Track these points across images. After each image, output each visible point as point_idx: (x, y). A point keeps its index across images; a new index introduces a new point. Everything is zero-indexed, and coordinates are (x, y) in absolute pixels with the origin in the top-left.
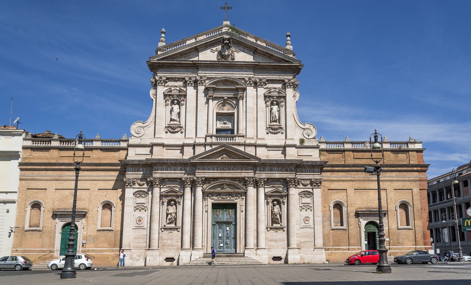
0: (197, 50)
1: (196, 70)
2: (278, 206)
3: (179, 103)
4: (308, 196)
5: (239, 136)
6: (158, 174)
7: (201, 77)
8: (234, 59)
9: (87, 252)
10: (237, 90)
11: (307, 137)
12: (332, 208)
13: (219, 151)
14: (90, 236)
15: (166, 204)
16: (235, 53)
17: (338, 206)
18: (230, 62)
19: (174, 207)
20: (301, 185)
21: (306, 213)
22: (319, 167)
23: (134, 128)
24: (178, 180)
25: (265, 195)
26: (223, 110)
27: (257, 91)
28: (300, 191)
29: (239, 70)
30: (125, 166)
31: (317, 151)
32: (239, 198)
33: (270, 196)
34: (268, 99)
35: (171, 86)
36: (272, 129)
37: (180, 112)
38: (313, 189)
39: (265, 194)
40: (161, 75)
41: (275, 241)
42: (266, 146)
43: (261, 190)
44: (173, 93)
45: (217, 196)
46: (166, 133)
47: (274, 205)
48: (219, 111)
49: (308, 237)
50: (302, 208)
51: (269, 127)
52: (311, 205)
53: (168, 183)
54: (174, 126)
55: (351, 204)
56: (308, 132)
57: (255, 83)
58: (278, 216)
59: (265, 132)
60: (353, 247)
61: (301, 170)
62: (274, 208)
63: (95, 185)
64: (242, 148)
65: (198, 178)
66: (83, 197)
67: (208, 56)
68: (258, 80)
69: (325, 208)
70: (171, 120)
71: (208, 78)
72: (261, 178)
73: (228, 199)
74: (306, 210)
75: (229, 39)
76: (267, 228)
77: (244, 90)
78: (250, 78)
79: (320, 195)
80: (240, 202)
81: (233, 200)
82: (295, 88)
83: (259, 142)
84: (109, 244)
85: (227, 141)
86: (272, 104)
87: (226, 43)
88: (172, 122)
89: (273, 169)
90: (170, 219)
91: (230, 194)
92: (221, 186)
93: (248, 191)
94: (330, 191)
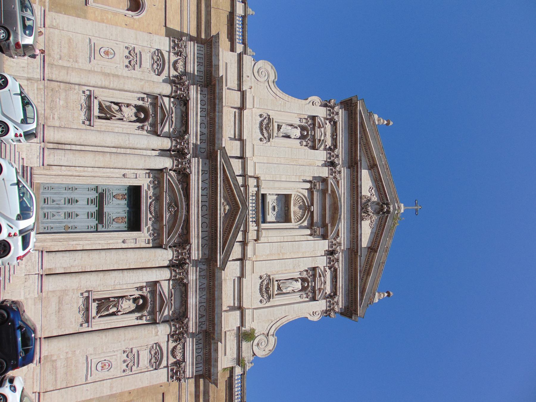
1: (347, 165)
2: (133, 306)
5: (258, 231)
6: (194, 95)
10: (324, 225)
11: (256, 342)
13: (235, 199)
15: (140, 103)
16: (369, 221)
19: (134, 118)
20: (174, 344)
22: (206, 371)
23: (266, 67)
24: (184, 128)
25: (156, 283)
26: (294, 205)
27: (322, 256)
28: (162, 345)
30: (208, 45)
32: (150, 235)
33: (153, 292)
34: (311, 273)
35: (325, 129)
36: (268, 284)
39: (158, 282)
40: (341, 116)
43: (166, 274)
44: (317, 130)
45: (154, 194)
46: (261, 116)
47: (135, 300)
48: (292, 199)
50: (128, 352)
51: (270, 279)
52: (134, 368)
53: (179, 110)
54: (271, 128)
56: (263, 344)
58: (114, 310)
59: (262, 274)
64: (240, 238)
65: (189, 162)
68: (336, 256)
71: (338, 182)
72: (187, 273)
73: (149, 216)
74: (125, 361)
75: (388, 212)
76: (88, 292)
77: (324, 237)
80: (144, 236)
81: (147, 225)
82: (326, 312)
83: (248, 264)
85: (250, 212)
86: (304, 280)
87: (382, 209)
89: (204, 293)
90: (109, 108)
91: (158, 218)
92: (174, 203)
93: (165, 251)
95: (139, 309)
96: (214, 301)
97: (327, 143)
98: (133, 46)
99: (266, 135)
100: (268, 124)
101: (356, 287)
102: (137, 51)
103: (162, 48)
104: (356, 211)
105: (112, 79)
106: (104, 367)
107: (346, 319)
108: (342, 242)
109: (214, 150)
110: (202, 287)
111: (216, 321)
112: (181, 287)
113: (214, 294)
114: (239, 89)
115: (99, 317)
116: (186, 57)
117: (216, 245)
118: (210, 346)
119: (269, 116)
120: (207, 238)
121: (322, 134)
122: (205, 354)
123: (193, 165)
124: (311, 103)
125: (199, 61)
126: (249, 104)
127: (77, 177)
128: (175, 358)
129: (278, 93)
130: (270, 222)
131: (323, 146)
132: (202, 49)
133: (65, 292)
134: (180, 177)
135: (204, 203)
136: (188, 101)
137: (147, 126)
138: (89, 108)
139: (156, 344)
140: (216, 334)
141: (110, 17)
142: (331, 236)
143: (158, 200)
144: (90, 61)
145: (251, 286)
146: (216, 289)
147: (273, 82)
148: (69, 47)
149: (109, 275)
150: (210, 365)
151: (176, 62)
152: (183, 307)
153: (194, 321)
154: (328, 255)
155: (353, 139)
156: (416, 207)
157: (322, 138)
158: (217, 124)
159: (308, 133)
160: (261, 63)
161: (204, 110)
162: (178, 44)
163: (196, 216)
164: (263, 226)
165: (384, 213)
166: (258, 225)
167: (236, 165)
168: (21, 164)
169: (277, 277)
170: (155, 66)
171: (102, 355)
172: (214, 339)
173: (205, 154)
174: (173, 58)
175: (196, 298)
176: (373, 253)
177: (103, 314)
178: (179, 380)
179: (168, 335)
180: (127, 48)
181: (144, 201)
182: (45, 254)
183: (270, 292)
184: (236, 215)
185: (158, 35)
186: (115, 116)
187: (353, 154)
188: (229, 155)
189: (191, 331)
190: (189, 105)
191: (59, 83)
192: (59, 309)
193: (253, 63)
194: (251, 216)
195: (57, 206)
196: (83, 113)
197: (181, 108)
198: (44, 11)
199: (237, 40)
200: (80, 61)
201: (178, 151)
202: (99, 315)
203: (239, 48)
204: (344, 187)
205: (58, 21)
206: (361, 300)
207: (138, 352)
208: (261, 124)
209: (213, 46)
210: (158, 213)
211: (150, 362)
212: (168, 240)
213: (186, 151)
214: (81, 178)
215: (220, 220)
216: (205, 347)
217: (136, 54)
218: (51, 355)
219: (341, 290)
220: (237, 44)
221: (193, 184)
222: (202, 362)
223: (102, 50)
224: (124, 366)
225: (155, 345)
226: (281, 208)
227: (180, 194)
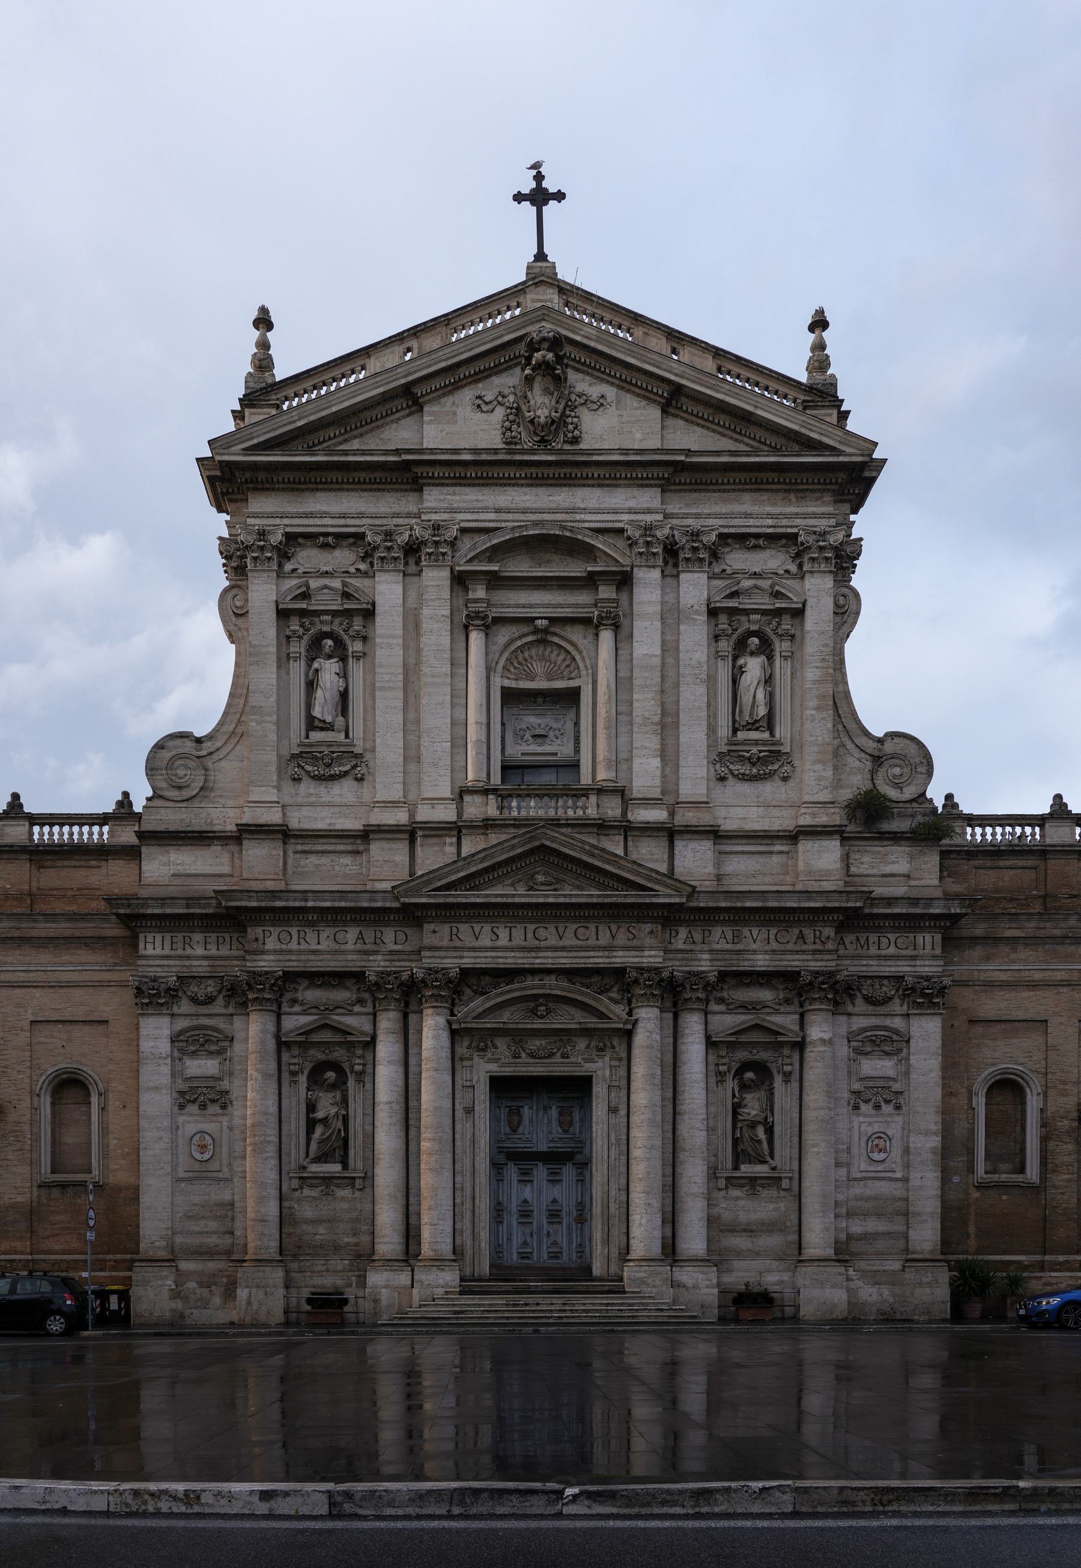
1: (412, 497)
3: (340, 653)
4: (887, 1049)
7: (437, 527)
8: (576, 440)
10: (591, 581)
12: (982, 1100)
15: (303, 1079)
17: (1007, 1087)
18: (560, 451)
20: (859, 1001)
24: (349, 983)
28: (855, 1027)
31: (931, 861)
36: (742, 759)
37: (346, 690)
38: (908, 1015)
39: (708, 1038)
41: (749, 1230)
42: (715, 834)
43: (693, 1026)
46: (297, 780)
47: (744, 1087)
49: (879, 1215)
52: (897, 1087)
55: (1064, 1083)
56: (897, 771)
57: (671, 551)
60: (1061, 1258)
61: (863, 937)
62: (742, 1099)
67: (464, 425)
69: (953, 1100)
70: (312, 724)
71: (464, 531)
73: (557, 1059)
74: (877, 1107)
77: (624, 581)
79: (939, 1044)
81: (578, 1064)
86: (741, 647)
88: (316, 736)
90: (321, 1142)
94: (978, 1029)
98: (175, 1095)
100: (315, 759)
102: (182, 1086)
106: (880, 1146)
112: (726, 987)
115: (772, 1158)
116: (178, 977)
119: (293, 756)
121: (326, 587)
122: (894, 929)
123: (438, 960)
124: (240, 622)
125: (180, 945)
127: (477, 1201)
128: (891, 998)
132: (150, 938)
133: (712, 1221)
134: (468, 991)
139: (849, 1041)
144: (226, 1180)
145: (744, 807)
149: (684, 1139)
151: (194, 1000)
153: (810, 957)
154: (676, 565)
161: (302, 934)
163: (560, 954)
167: (433, 857)
169: (724, 730)
170: (213, 1048)
171: (855, 1151)
173: (408, 931)
174: (185, 1006)
176: (684, 400)
177: (767, 1152)
178: (942, 991)
179: (833, 1014)
180: (182, 1107)
181: (525, 1069)
186: (339, 1130)
191: (284, 1236)
192: (745, 1230)
196: (341, 1193)
197: (301, 988)
200: (228, 1198)
201: (406, 994)
202: (768, 1159)
207: (861, 1079)
211: (887, 1054)
213: (405, 976)
214: (477, 1195)
216: (877, 929)
218: (836, 1243)
219: (785, 522)
223: (198, 1156)
224: (887, 1109)
225: (853, 1044)
227: (509, 991)
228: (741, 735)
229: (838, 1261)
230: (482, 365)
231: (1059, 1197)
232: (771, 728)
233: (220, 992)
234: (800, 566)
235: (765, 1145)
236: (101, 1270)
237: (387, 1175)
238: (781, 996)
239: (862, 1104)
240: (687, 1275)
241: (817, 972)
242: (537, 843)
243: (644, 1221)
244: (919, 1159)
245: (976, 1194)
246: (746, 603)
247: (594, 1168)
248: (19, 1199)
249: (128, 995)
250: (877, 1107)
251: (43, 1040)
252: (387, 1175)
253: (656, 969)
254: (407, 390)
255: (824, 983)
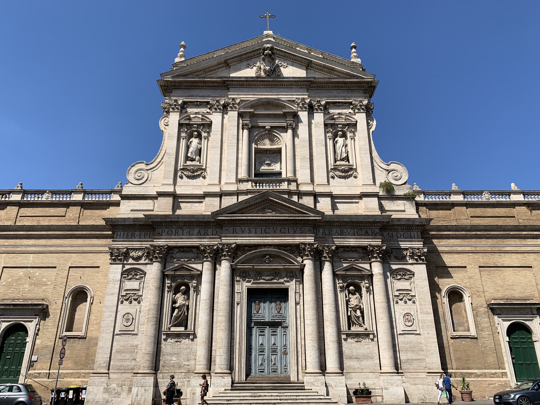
0: (228, 65)
2: (357, 295)
3: (199, 136)
9: (36, 377)
10: (285, 115)
14: (46, 347)
21: (405, 306)
24: (194, 250)
29: (286, 89)
36: (339, 170)
49: (412, 351)
52: (412, 293)
56: (395, 175)
61: (390, 233)
62: (350, 298)
63: (66, 260)
64: (295, 198)
66: (44, 280)
68: (314, 103)
70: (187, 158)
74: (406, 302)
75: (272, 49)
78: (303, 99)
80: (292, 285)
81: (282, 283)
84: (75, 363)
85: (271, 188)
88: (189, 163)
89: (345, 230)
90: (177, 318)
91: (276, 274)
95: (358, 289)
96: (352, 222)
97: (205, 112)
99: (199, 173)
101: (345, 83)
102: (124, 293)
103: (120, 271)
104: (271, 83)
105: (151, 316)
107: (376, 91)
108: (301, 97)
109: (214, 222)
110: (339, 232)
111: (372, 220)
112: (339, 252)
113: (346, 222)
114: (156, 198)
116: (127, 249)
117: (301, 220)
118: (395, 225)
120: (295, 228)
121: (196, 117)
124: (166, 127)
126: (170, 189)
129: (158, 160)
130: (281, 169)
131: (207, 116)
132: (119, 234)
134: (240, 253)
135: (263, 231)
136: (169, 246)
137: (194, 283)
138: (178, 335)
140: (383, 220)
141: (94, 317)
142: (294, 108)
143: (260, 273)
144: (136, 334)
146: (342, 220)
147: (147, 165)
148: (124, 352)
150: (412, 225)
152: (358, 249)
154: (313, 111)
155: (201, 84)
156: (268, 17)
157: (200, 116)
158: (190, 220)
159: (195, 131)
160: (131, 177)
162: (116, 256)
164: (284, 176)
165: (273, 53)
166: (284, 181)
167: (228, 201)
168: (230, 392)
170: (138, 277)
172: (388, 222)
173: (218, 230)
175: (349, 238)
176: (313, 65)
182: (307, 371)
183: (346, 168)
184: (274, 201)
185: (108, 274)
187: (215, 84)
188: (218, 209)
189: (381, 243)
190: (172, 245)
192: (356, 358)
193: (130, 185)
194: (275, 188)
195: (266, 361)
198: (94, 373)
199: (108, 199)
200: (136, 343)
201: (215, 254)
203: (116, 197)
204: (247, 95)
205: (101, 362)
206: (358, 77)
208: (189, 177)
209: (116, 223)
210: (272, 272)
211: (407, 280)
212: (297, 264)
213: (215, 247)
215: (278, 216)
216: (396, 230)
217: (127, 294)
220: (112, 199)
221: (245, 241)
222: (409, 233)
226: (267, 157)
228: (338, 163)
229: (398, 373)
230: (249, 55)
231: (487, 342)
232: (348, 161)
233: (143, 254)
234: (354, 111)
235: (361, 319)
236: (78, 378)
237: (202, 332)
238: (361, 256)
239: (399, 301)
240: (331, 380)
241: (375, 246)
242: (265, 198)
243: (312, 354)
244: (425, 325)
245: (452, 341)
246: (338, 121)
247: (290, 329)
248: (49, 344)
249: (108, 256)
250: (406, 302)
251: (73, 274)
252: (202, 332)
253: (311, 244)
254: (226, 61)
255: (377, 250)
